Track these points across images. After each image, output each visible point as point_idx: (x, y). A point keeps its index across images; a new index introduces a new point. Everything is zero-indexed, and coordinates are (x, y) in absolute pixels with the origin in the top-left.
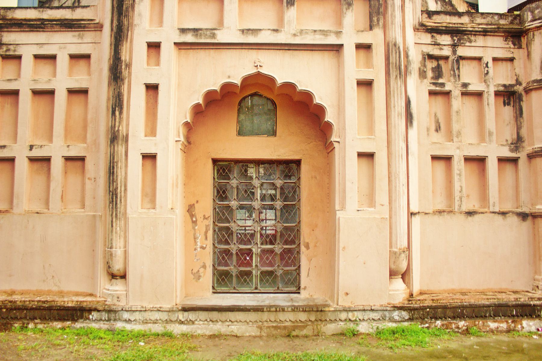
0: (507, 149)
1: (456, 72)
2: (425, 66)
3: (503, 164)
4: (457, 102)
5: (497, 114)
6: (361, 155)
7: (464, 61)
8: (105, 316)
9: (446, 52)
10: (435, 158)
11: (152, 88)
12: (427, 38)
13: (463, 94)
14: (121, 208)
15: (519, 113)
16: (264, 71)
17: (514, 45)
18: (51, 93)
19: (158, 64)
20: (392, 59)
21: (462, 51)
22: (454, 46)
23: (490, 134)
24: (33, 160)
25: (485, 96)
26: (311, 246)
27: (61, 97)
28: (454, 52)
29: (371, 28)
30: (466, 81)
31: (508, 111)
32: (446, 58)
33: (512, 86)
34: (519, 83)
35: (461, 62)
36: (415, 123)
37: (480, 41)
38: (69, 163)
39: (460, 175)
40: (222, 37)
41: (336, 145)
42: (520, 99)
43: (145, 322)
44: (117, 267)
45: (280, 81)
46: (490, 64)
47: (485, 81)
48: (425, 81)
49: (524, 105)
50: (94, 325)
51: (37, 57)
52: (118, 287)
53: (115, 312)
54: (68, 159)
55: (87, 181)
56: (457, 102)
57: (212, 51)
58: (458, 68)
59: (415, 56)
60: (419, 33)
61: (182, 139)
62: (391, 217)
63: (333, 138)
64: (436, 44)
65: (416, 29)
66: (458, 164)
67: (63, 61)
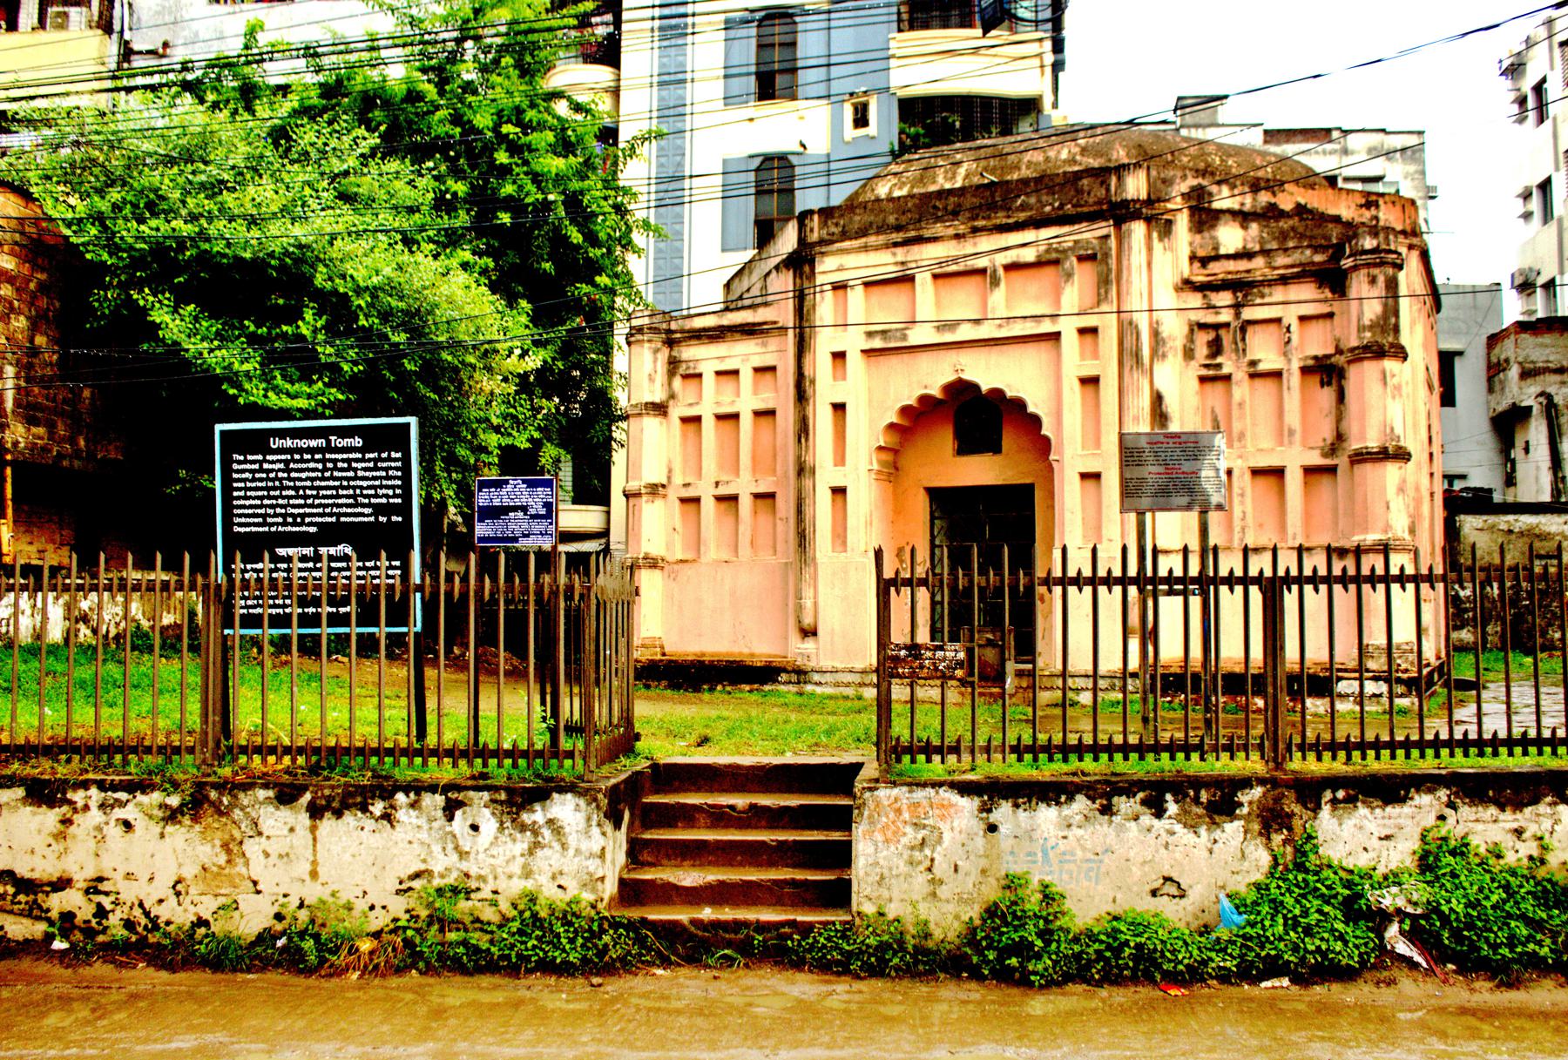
0: (1317, 453)
1: (1240, 345)
2: (1192, 341)
3: (1314, 478)
4: (1241, 389)
5: (1305, 402)
6: (1084, 476)
7: (1257, 328)
8: (794, 678)
9: (1226, 316)
11: (839, 408)
12: (1195, 300)
13: (1253, 376)
14: (810, 553)
15: (1341, 397)
16: (966, 376)
17: (1333, 292)
18: (735, 417)
19: (844, 378)
20: (1127, 344)
21: (1248, 314)
22: (1237, 307)
23: (1291, 432)
24: (720, 499)
25: (1285, 375)
27: (746, 420)
28: (1238, 315)
29: (1099, 304)
30: (1256, 357)
31: (1327, 396)
32: (1227, 325)
34: (1339, 351)
35: (1250, 330)
37: (1278, 294)
38: (759, 502)
39: (1242, 495)
40: (917, 336)
43: (837, 685)
44: (808, 621)
45: (985, 388)
47: (1285, 354)
48: (1194, 364)
50: (782, 688)
51: (718, 373)
52: (809, 645)
53: (805, 673)
54: (757, 496)
56: (1241, 389)
57: (906, 357)
58: (1243, 339)
59: (1174, 329)
60: (1184, 295)
61: (875, 466)
63: (1052, 457)
64: (1210, 307)
65: (1178, 289)
67: (746, 376)
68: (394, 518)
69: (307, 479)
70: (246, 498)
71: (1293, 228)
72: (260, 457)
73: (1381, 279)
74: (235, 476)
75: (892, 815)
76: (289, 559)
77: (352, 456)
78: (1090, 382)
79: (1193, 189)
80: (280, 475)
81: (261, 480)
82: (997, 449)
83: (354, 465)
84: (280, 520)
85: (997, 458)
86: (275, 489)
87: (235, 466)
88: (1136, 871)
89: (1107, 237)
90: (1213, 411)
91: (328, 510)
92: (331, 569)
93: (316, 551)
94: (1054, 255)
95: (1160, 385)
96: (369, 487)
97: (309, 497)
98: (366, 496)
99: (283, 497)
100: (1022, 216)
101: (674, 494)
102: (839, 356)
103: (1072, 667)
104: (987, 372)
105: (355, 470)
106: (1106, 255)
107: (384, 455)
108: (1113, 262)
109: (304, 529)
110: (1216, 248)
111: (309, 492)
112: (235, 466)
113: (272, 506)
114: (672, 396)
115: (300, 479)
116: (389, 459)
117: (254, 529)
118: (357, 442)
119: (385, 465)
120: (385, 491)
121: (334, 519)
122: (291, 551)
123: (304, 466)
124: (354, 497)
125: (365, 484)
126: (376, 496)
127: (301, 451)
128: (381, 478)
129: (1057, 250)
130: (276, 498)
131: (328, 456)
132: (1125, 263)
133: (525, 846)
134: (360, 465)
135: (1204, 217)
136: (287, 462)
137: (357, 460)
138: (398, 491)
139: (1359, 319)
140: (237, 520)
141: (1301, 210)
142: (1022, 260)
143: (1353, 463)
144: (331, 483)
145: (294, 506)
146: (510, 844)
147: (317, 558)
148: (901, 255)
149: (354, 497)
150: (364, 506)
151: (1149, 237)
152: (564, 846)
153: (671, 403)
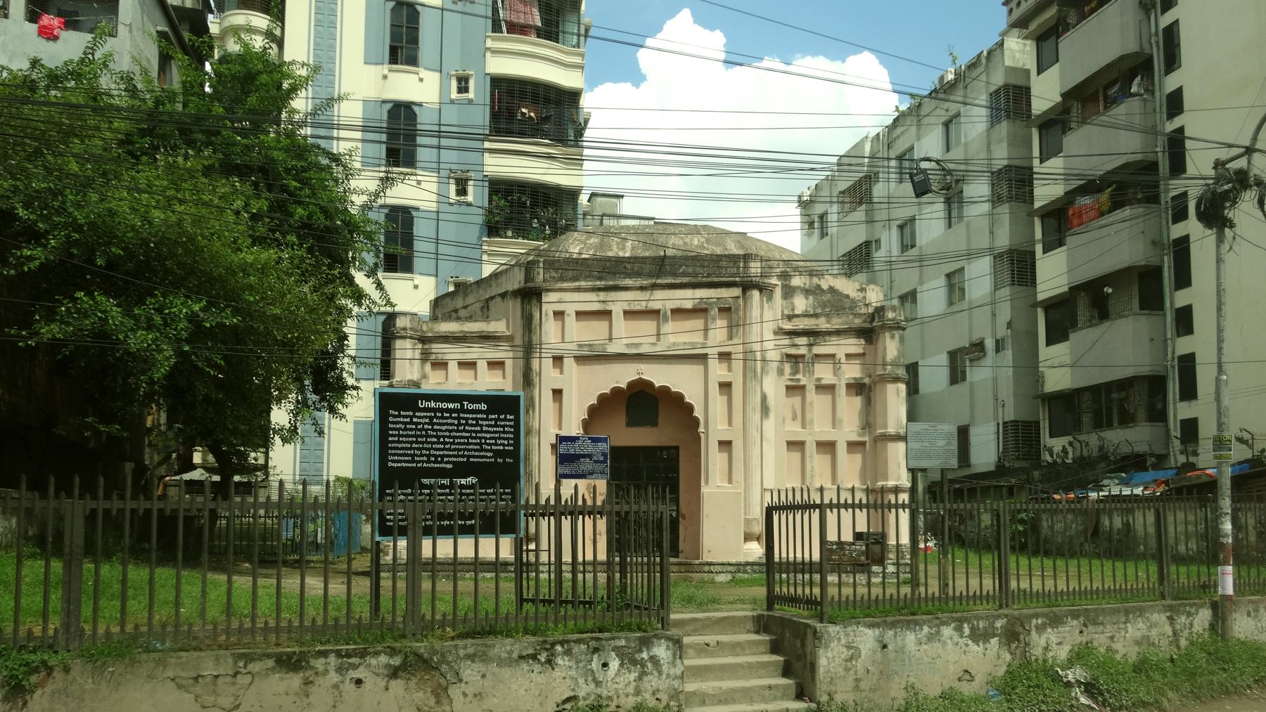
6: (721, 443)
9: (803, 351)
11: (557, 393)
21: (817, 350)
22: (810, 345)
25: (837, 388)
26: (687, 517)
28: (810, 351)
32: (803, 356)
33: (861, 378)
36: (772, 415)
40: (613, 349)
41: (702, 435)
42: (870, 390)
45: (657, 385)
49: (872, 395)
56: (811, 394)
59: (773, 355)
62: (745, 492)
65: (776, 333)
66: (811, 448)
67: (482, 365)
68: (508, 460)
69: (446, 431)
70: (399, 442)
71: (829, 301)
72: (411, 413)
73: (897, 336)
74: (390, 426)
75: (836, 642)
76: (430, 487)
77: (479, 416)
78: (726, 387)
80: (426, 426)
81: (411, 430)
82: (654, 423)
83: (481, 422)
84: (425, 459)
85: (654, 429)
86: (421, 436)
87: (391, 419)
88: (952, 668)
89: (738, 297)
90: (793, 406)
91: (460, 453)
92: (461, 494)
93: (451, 482)
94: (704, 306)
96: (490, 438)
97: (447, 443)
98: (488, 444)
99: (428, 443)
100: (685, 280)
102: (558, 360)
103: (813, 559)
104: (659, 376)
105: (481, 426)
106: (737, 309)
107: (503, 416)
108: (741, 313)
109: (442, 466)
110: (793, 310)
111: (447, 440)
112: (391, 419)
113: (418, 449)
114: (424, 376)
115: (441, 431)
116: (505, 420)
117: (404, 465)
118: (483, 407)
119: (502, 423)
120: (502, 441)
121: (465, 459)
122: (433, 481)
123: (444, 421)
124: (480, 444)
125: (488, 436)
126: (496, 444)
127: (442, 411)
128: (499, 432)
129: (706, 303)
130: (422, 443)
131: (461, 415)
132: (748, 315)
133: (637, 674)
134: (485, 423)
135: (789, 292)
136: (431, 418)
137: (483, 419)
138: (511, 442)
139: (884, 358)
140: (390, 458)
141: (832, 290)
142: (683, 307)
144: (464, 434)
145: (436, 449)
146: (627, 675)
147: (452, 486)
148: (602, 296)
149: (480, 444)
150: (487, 451)
151: (762, 301)
152: (660, 673)
153: (423, 381)
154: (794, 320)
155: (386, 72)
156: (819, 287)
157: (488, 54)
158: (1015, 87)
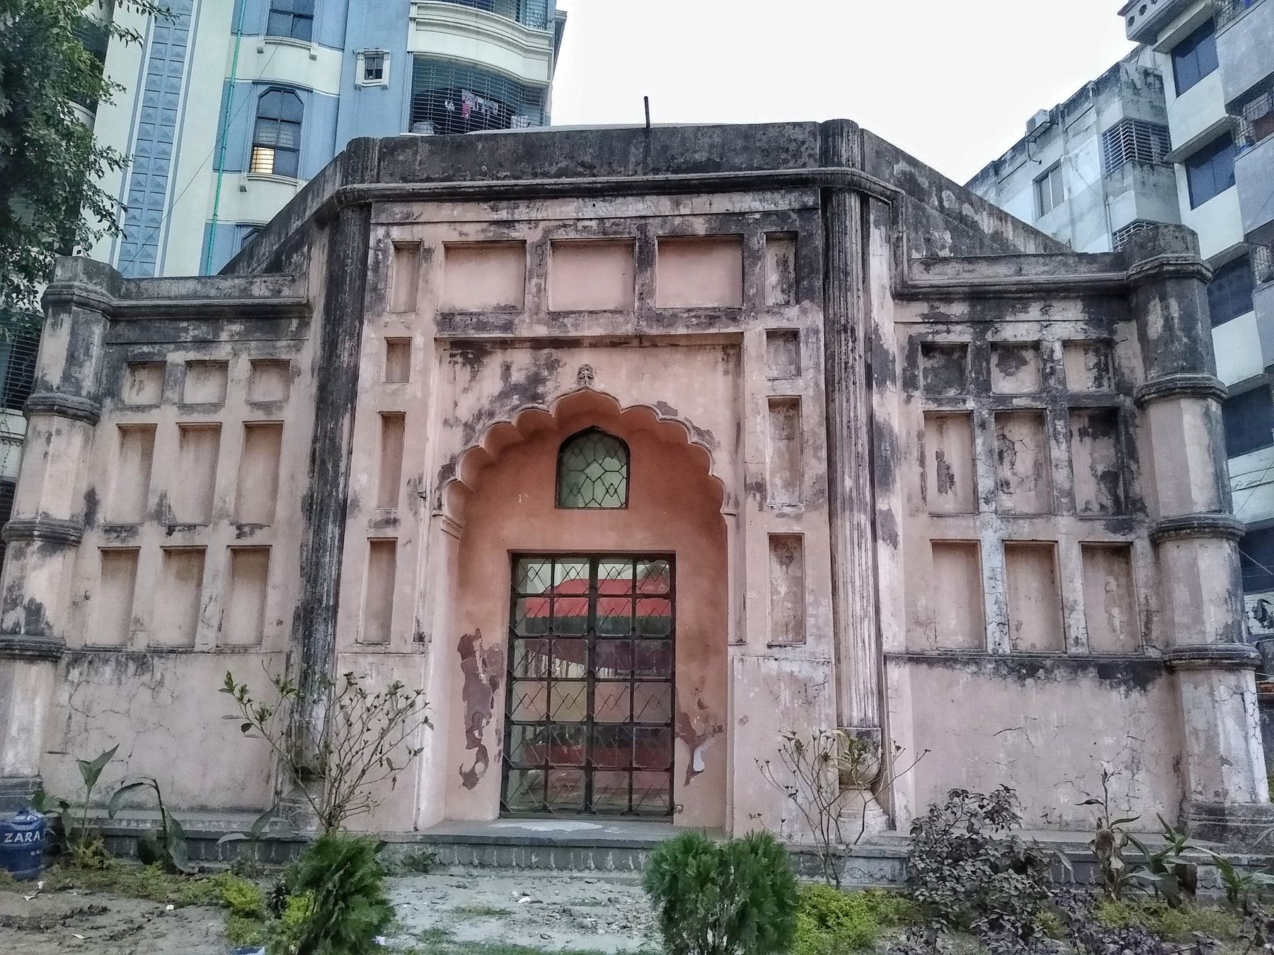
0: (1099, 526)
6: (777, 541)
9: (961, 335)
10: (940, 546)
11: (393, 421)
12: (917, 310)
16: (599, 385)
19: (405, 378)
32: (963, 347)
38: (241, 559)
41: (729, 521)
45: (625, 403)
46: (1058, 354)
49: (1139, 434)
55: (270, 591)
66: (992, 559)
78: (787, 407)
79: (904, 173)
95: (880, 415)
101: (94, 541)
143: (1156, 542)
153: (108, 402)
154: (938, 268)
155: (262, 45)
156: (974, 225)
157: (412, 25)
158: (1139, 124)
